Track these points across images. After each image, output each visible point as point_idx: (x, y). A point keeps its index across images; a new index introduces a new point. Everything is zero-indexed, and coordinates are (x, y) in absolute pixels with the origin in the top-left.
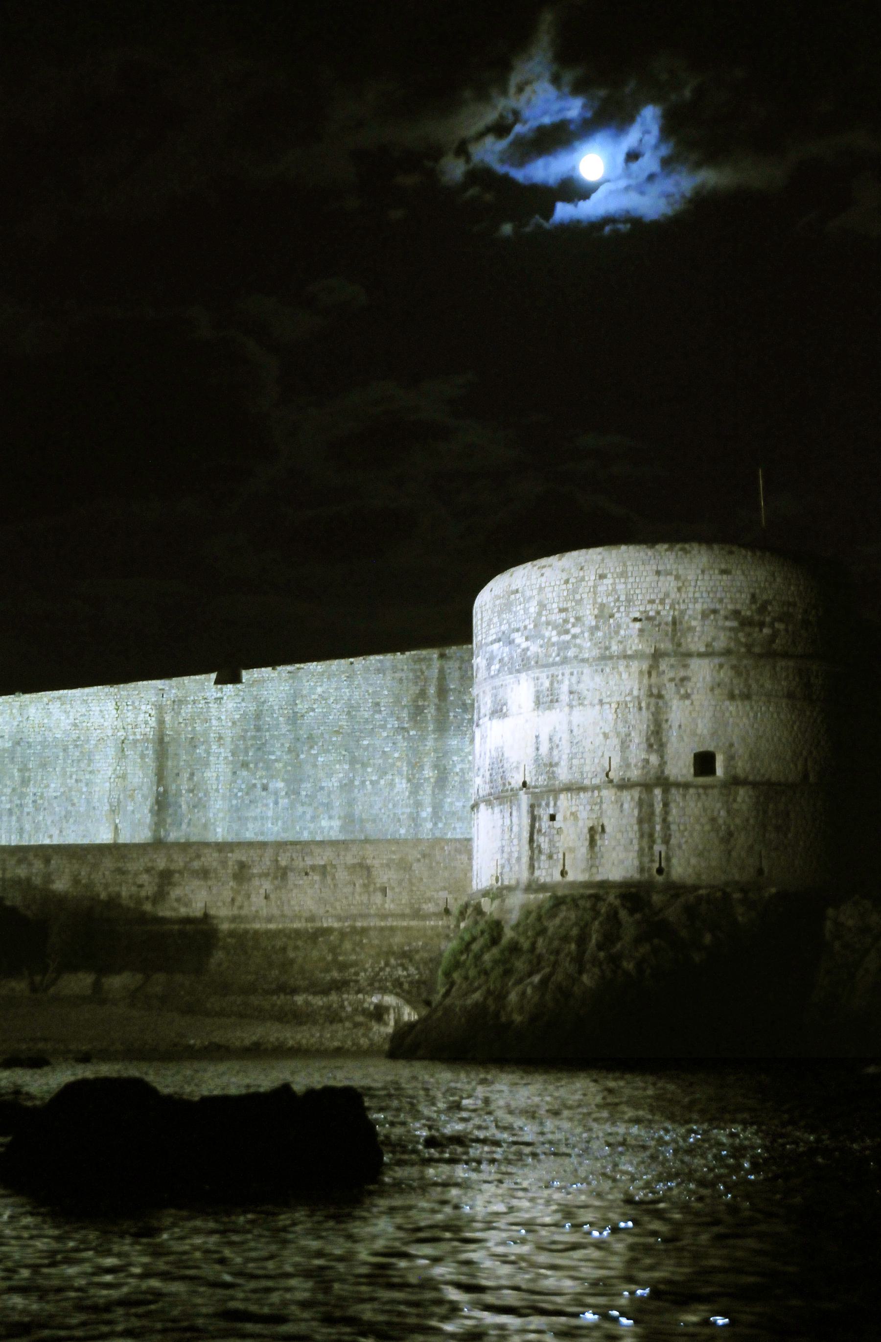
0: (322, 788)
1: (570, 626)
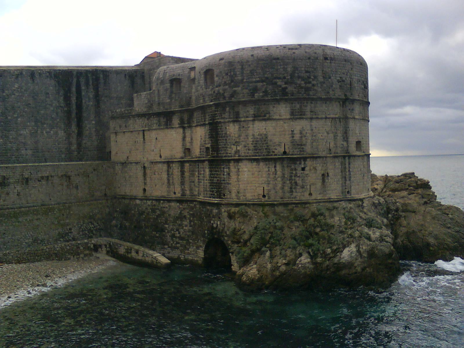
0: (21, 135)
1: (311, 80)
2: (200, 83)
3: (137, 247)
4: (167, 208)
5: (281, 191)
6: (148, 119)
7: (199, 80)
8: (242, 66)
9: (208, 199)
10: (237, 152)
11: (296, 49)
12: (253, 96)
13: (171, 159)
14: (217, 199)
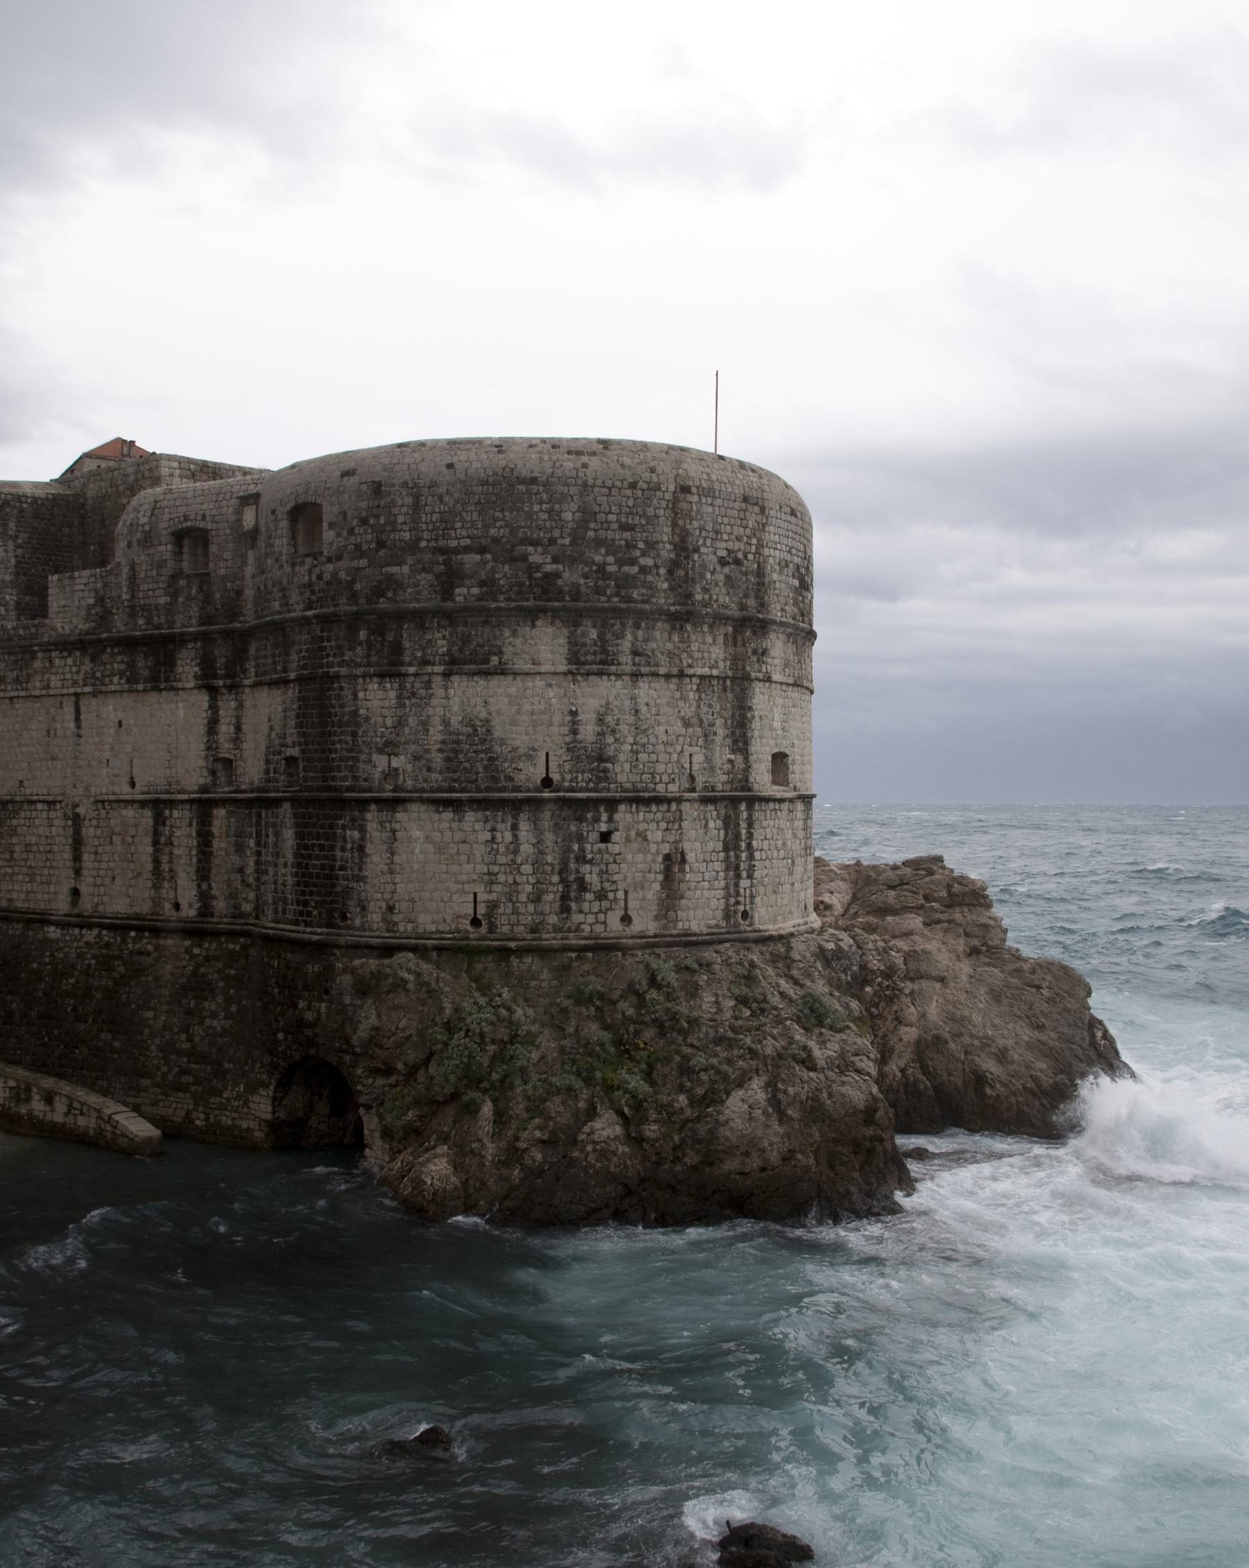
1: (638, 553)
2: (272, 546)
3: (48, 1082)
4: (149, 954)
5: (531, 908)
6: (93, 660)
7: (270, 537)
8: (417, 497)
9: (288, 927)
10: (392, 773)
11: (594, 454)
12: (447, 594)
13: (167, 792)
14: (319, 930)
